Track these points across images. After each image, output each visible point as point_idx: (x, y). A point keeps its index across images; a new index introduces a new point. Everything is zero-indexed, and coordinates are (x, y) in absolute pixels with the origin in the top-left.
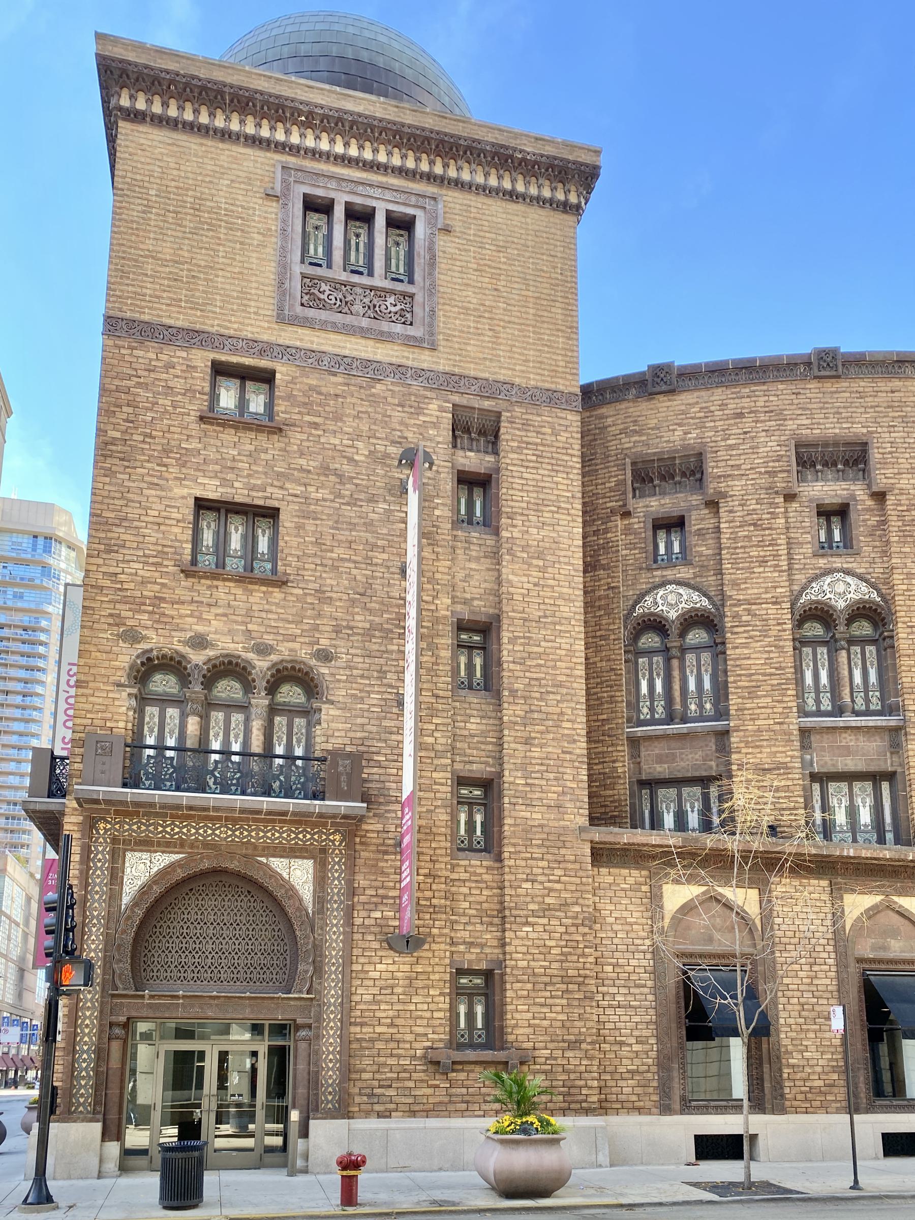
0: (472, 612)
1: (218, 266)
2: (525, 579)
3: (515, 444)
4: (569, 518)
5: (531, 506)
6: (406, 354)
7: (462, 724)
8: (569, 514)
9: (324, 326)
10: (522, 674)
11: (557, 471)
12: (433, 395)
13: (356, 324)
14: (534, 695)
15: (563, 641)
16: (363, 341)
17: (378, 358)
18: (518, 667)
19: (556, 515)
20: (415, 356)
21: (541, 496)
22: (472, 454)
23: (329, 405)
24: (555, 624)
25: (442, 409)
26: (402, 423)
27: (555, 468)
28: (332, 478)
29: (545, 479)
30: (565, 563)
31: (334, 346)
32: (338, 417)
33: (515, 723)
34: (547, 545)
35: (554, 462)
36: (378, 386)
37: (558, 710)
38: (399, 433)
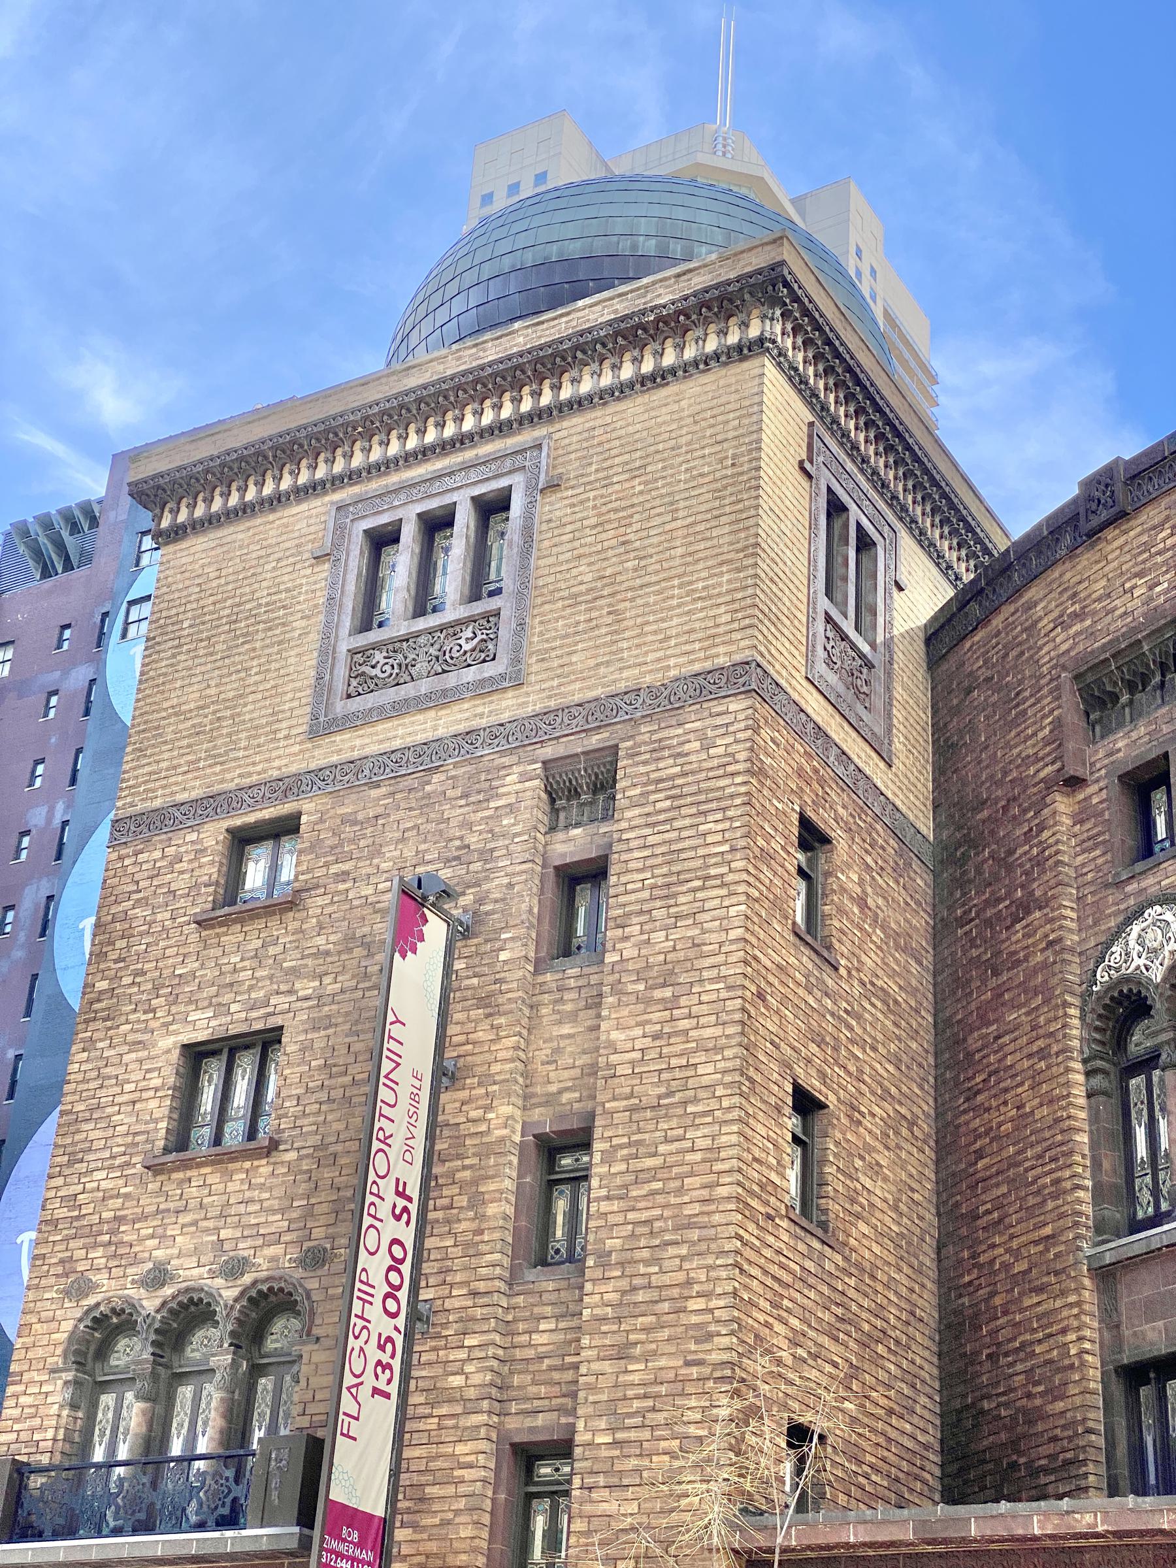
0: (562, 1117)
1: (248, 690)
2: (638, 1032)
3: (638, 791)
4: (724, 892)
5: (656, 892)
6: (480, 710)
7: (526, 1337)
8: (723, 885)
9: (401, 709)
10: (619, 1219)
11: (705, 813)
12: (515, 759)
13: (412, 693)
14: (638, 1255)
15: (699, 1136)
16: (420, 717)
17: (441, 732)
18: (615, 1206)
19: (700, 895)
20: (493, 707)
21: (676, 868)
22: (577, 832)
23: (364, 837)
24: (685, 1103)
25: (525, 778)
26: (461, 826)
27: (703, 807)
28: (358, 952)
29: (685, 834)
30: (711, 980)
31: (381, 742)
32: (376, 851)
33: (604, 1319)
34: (681, 955)
35: (702, 797)
36: (436, 778)
37: (681, 1277)
38: (457, 843)
